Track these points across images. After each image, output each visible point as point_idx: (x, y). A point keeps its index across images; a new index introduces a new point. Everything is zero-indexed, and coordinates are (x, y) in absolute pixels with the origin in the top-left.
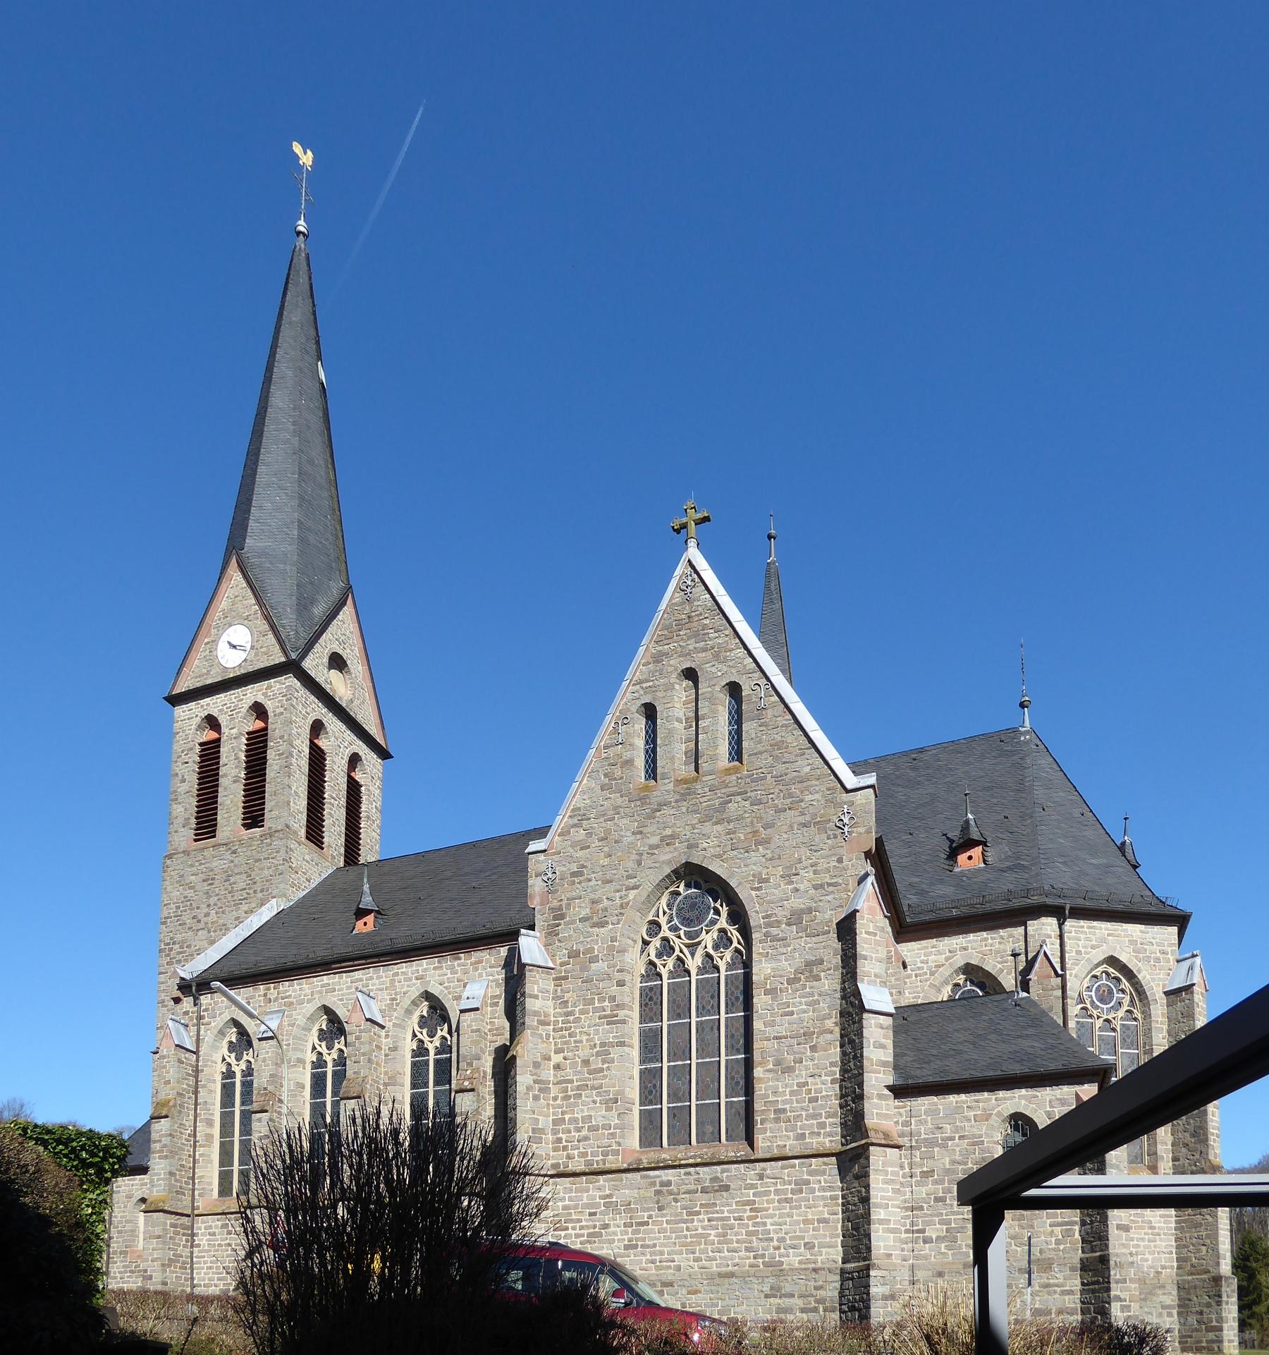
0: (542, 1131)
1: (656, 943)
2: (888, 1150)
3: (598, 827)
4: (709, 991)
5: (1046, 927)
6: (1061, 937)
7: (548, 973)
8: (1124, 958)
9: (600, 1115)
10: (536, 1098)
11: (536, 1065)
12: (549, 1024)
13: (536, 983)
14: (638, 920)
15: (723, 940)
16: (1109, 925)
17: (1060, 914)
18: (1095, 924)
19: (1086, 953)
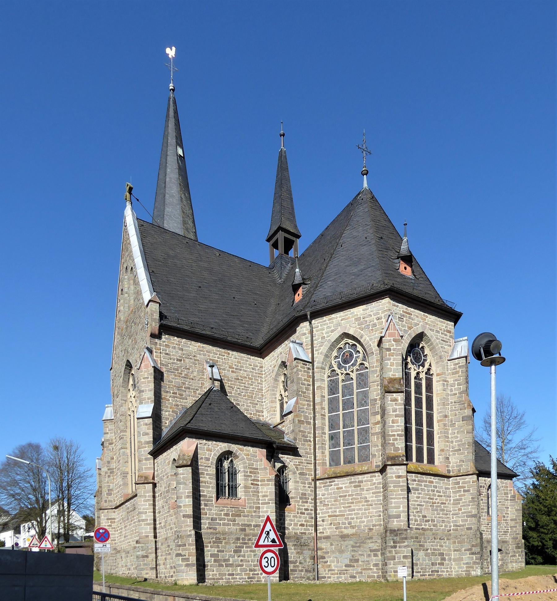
0: (112, 490)
2: (146, 485)
6: (312, 332)
7: (112, 422)
8: (351, 332)
10: (109, 476)
11: (109, 462)
12: (112, 444)
13: (108, 427)
14: (124, 391)
16: (341, 314)
17: (303, 318)
18: (333, 316)
19: (328, 337)
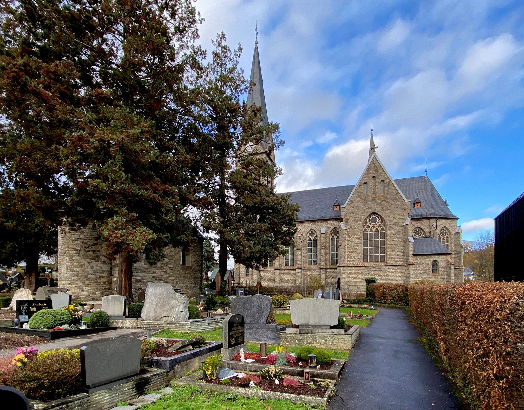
1: (366, 225)
3: (356, 204)
4: (377, 235)
5: (433, 221)
9: (356, 256)
15: (380, 226)
